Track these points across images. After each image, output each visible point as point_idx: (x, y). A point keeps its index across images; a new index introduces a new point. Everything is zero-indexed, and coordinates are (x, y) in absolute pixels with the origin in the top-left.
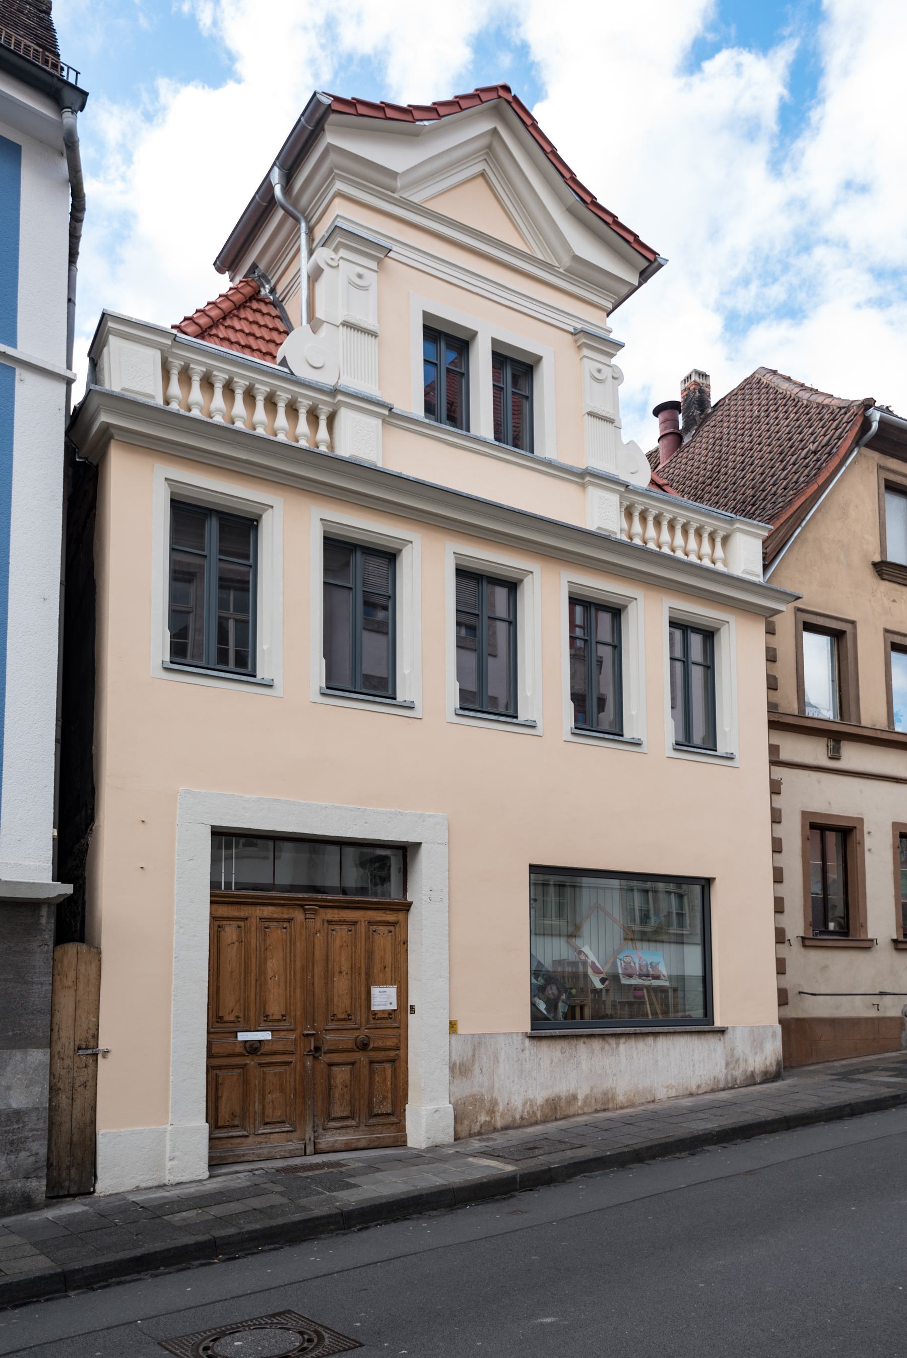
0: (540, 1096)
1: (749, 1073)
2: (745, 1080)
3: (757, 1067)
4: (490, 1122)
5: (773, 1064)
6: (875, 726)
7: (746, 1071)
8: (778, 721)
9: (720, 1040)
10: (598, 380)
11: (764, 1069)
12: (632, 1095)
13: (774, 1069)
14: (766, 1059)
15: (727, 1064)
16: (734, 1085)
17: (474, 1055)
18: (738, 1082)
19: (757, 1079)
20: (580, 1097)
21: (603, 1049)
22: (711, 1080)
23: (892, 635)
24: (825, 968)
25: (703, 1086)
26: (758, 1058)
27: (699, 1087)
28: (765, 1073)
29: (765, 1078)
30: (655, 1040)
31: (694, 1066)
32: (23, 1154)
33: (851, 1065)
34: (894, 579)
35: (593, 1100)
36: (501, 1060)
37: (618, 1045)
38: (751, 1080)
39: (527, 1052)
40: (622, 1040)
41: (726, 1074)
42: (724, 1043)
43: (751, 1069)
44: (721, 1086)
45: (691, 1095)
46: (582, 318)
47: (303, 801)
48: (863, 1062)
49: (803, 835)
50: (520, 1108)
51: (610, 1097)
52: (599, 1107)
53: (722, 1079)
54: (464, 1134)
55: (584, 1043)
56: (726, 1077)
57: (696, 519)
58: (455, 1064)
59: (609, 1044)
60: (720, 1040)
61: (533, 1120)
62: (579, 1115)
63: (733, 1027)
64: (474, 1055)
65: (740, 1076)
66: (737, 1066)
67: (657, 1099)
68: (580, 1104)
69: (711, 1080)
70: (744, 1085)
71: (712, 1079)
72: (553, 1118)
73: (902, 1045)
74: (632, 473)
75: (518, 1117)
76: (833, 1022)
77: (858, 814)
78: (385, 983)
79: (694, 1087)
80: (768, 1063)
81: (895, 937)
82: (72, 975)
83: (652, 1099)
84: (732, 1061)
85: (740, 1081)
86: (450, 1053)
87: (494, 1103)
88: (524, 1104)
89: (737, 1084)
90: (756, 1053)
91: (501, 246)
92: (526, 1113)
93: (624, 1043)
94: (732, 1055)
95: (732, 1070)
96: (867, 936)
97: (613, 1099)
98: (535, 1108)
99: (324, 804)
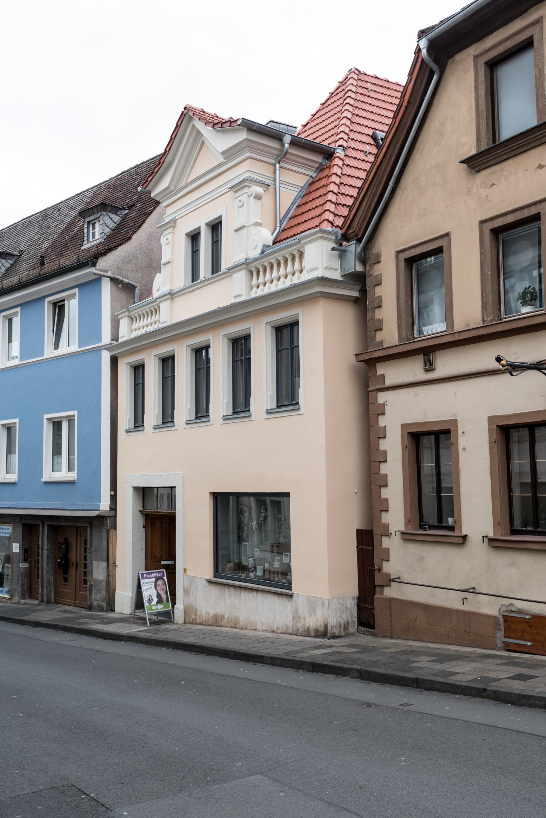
0: (212, 612)
1: (306, 628)
2: (304, 632)
3: (311, 625)
4: (195, 619)
5: (322, 626)
6: (468, 325)
7: (305, 626)
8: (371, 358)
9: (290, 601)
10: (242, 205)
11: (316, 628)
12: (246, 623)
13: (323, 629)
14: (317, 621)
15: (293, 618)
16: (297, 633)
17: (190, 586)
18: (300, 632)
19: (311, 633)
20: (226, 617)
21: (234, 593)
22: (284, 626)
23: (491, 222)
24: (422, 558)
25: (280, 628)
26: (312, 619)
27: (278, 628)
28: (317, 631)
29: (316, 634)
30: (257, 593)
31: (275, 614)
32: (102, 594)
33: (448, 650)
34: (487, 165)
35: (231, 621)
36: (199, 590)
37: (241, 592)
38: (307, 633)
39: (207, 588)
40: (242, 591)
41: (293, 625)
42: (292, 604)
43: (307, 625)
44: (290, 631)
45: (274, 632)
46: (235, 176)
47: (148, 474)
48: (426, 647)
49: (402, 444)
50: (204, 616)
51: (237, 621)
52: (233, 625)
53: (291, 627)
54: (187, 622)
55: (227, 588)
56: (293, 627)
57: (286, 253)
58: (185, 588)
59: (237, 591)
60: (290, 601)
61: (209, 623)
62: (225, 626)
63: (297, 594)
64: (190, 586)
65: (301, 628)
66: (299, 621)
67: (257, 629)
68: (225, 621)
69: (284, 626)
70: (304, 635)
71: (285, 625)
72: (216, 625)
73: (497, 645)
74: (255, 249)
75: (204, 620)
76: (427, 608)
77: (453, 416)
78: (16, 553)
79: (275, 628)
80: (319, 625)
81: (491, 535)
82: (112, 539)
83: (255, 628)
84: (296, 617)
85: (301, 632)
86: (183, 583)
87: (196, 611)
88: (206, 614)
89: (299, 633)
90: (311, 615)
91: (199, 178)
92: (206, 619)
93: (243, 592)
94: (297, 613)
95: (296, 623)
96: (461, 532)
97: (239, 623)
98: (210, 618)
99: (153, 474)
